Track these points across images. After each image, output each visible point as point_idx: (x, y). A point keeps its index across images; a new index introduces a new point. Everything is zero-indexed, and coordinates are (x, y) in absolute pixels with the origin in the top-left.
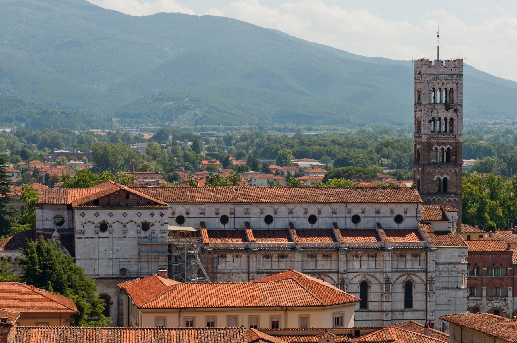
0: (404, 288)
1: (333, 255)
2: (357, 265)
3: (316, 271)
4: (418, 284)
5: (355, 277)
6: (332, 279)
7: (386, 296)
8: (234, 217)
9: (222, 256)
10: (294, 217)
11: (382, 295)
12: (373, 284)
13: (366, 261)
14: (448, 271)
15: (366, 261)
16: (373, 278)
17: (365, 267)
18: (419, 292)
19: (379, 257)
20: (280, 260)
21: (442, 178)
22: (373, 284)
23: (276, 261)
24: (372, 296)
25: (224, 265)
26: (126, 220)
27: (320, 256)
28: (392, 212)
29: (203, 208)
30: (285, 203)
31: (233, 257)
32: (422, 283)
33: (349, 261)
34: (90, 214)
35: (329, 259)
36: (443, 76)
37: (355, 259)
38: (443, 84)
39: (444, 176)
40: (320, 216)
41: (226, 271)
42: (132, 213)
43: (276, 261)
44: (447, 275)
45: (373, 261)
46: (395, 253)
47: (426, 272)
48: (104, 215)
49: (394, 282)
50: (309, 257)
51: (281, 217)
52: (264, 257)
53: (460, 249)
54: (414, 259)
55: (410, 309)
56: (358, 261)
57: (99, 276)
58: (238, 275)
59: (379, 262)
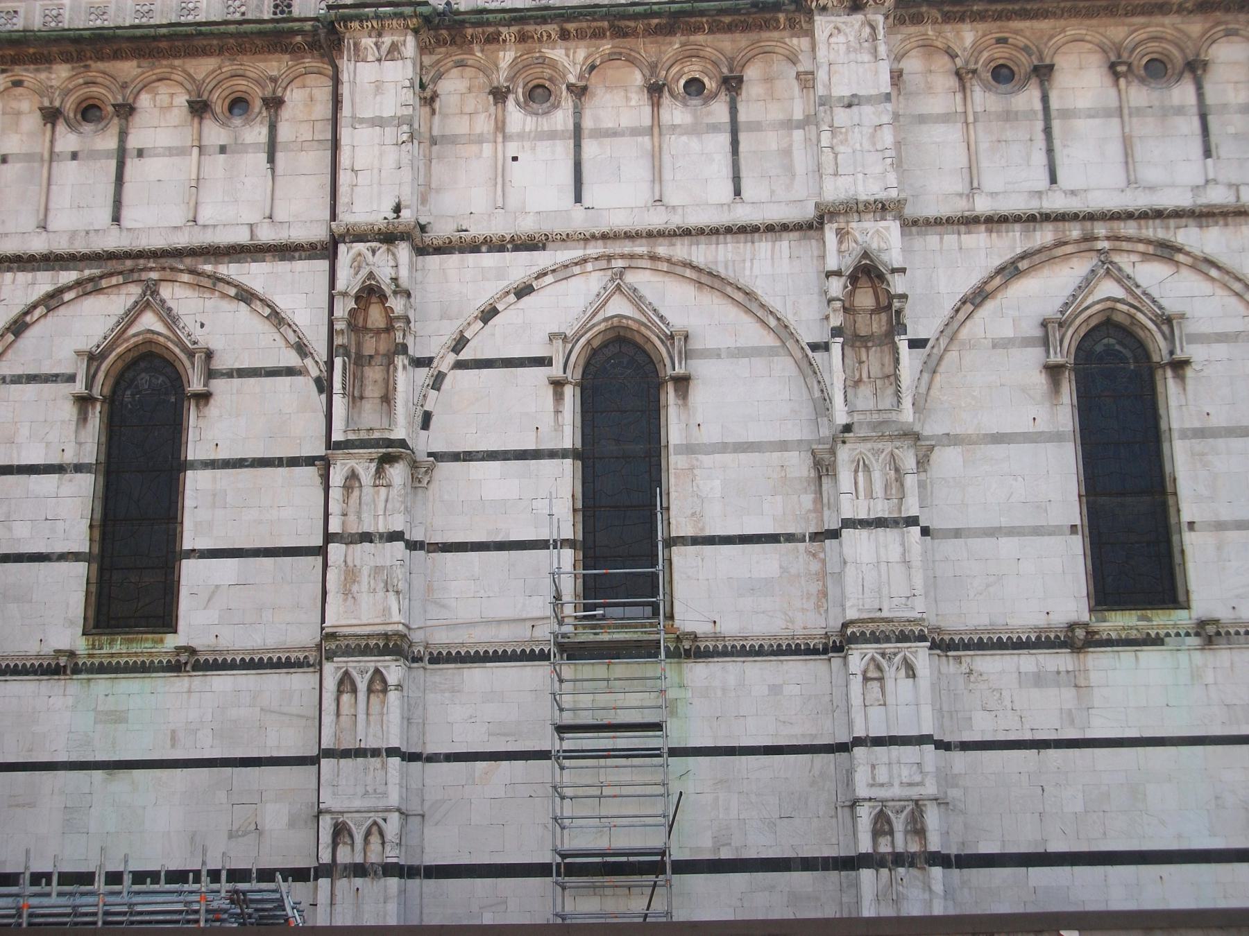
1: (295, 97)
3: (113, 241)
4: (1220, 350)
5: (523, 291)
6: (276, 318)
7: (862, 466)
11: (823, 468)
12: (716, 354)
13: (635, 132)
15: (635, 132)
19: (772, 96)
22: (716, 354)
33: (453, 140)
35: (257, 134)
37: (516, 117)
45: (694, 130)
46: (927, 47)
50: (51, 116)
54: (1138, 95)
55: (1161, 620)
56: (552, 135)
59: (772, 140)
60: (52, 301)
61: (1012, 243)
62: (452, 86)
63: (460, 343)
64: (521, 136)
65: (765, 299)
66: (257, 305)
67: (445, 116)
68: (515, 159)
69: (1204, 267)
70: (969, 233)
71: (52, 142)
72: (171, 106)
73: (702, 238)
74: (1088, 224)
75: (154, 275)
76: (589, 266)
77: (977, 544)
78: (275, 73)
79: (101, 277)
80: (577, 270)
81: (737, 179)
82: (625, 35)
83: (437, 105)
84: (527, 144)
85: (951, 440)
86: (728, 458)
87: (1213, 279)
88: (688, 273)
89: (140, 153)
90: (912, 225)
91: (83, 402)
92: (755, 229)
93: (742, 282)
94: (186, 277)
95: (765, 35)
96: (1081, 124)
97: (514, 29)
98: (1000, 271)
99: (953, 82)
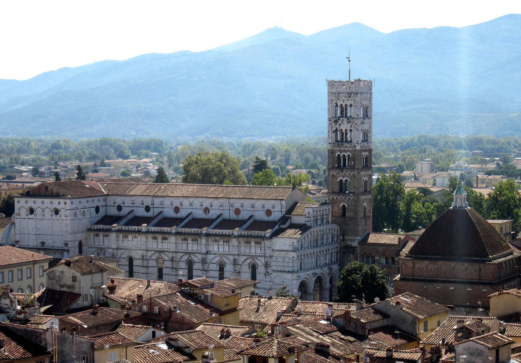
0: (251, 269)
2: (216, 248)
3: (187, 251)
8: (154, 207)
9: (126, 237)
17: (221, 250)
18: (261, 273)
20: (163, 241)
21: (344, 180)
24: (227, 274)
25: (126, 243)
26: (44, 206)
29: (133, 199)
30: (187, 197)
31: (132, 237)
34: (23, 200)
36: (343, 94)
38: (343, 100)
39: (345, 179)
40: (211, 208)
41: (127, 248)
42: (47, 201)
44: (281, 260)
45: (226, 245)
48: (31, 202)
49: (243, 263)
50: (182, 240)
53: (290, 239)
57: (29, 247)
62: (210, 240)
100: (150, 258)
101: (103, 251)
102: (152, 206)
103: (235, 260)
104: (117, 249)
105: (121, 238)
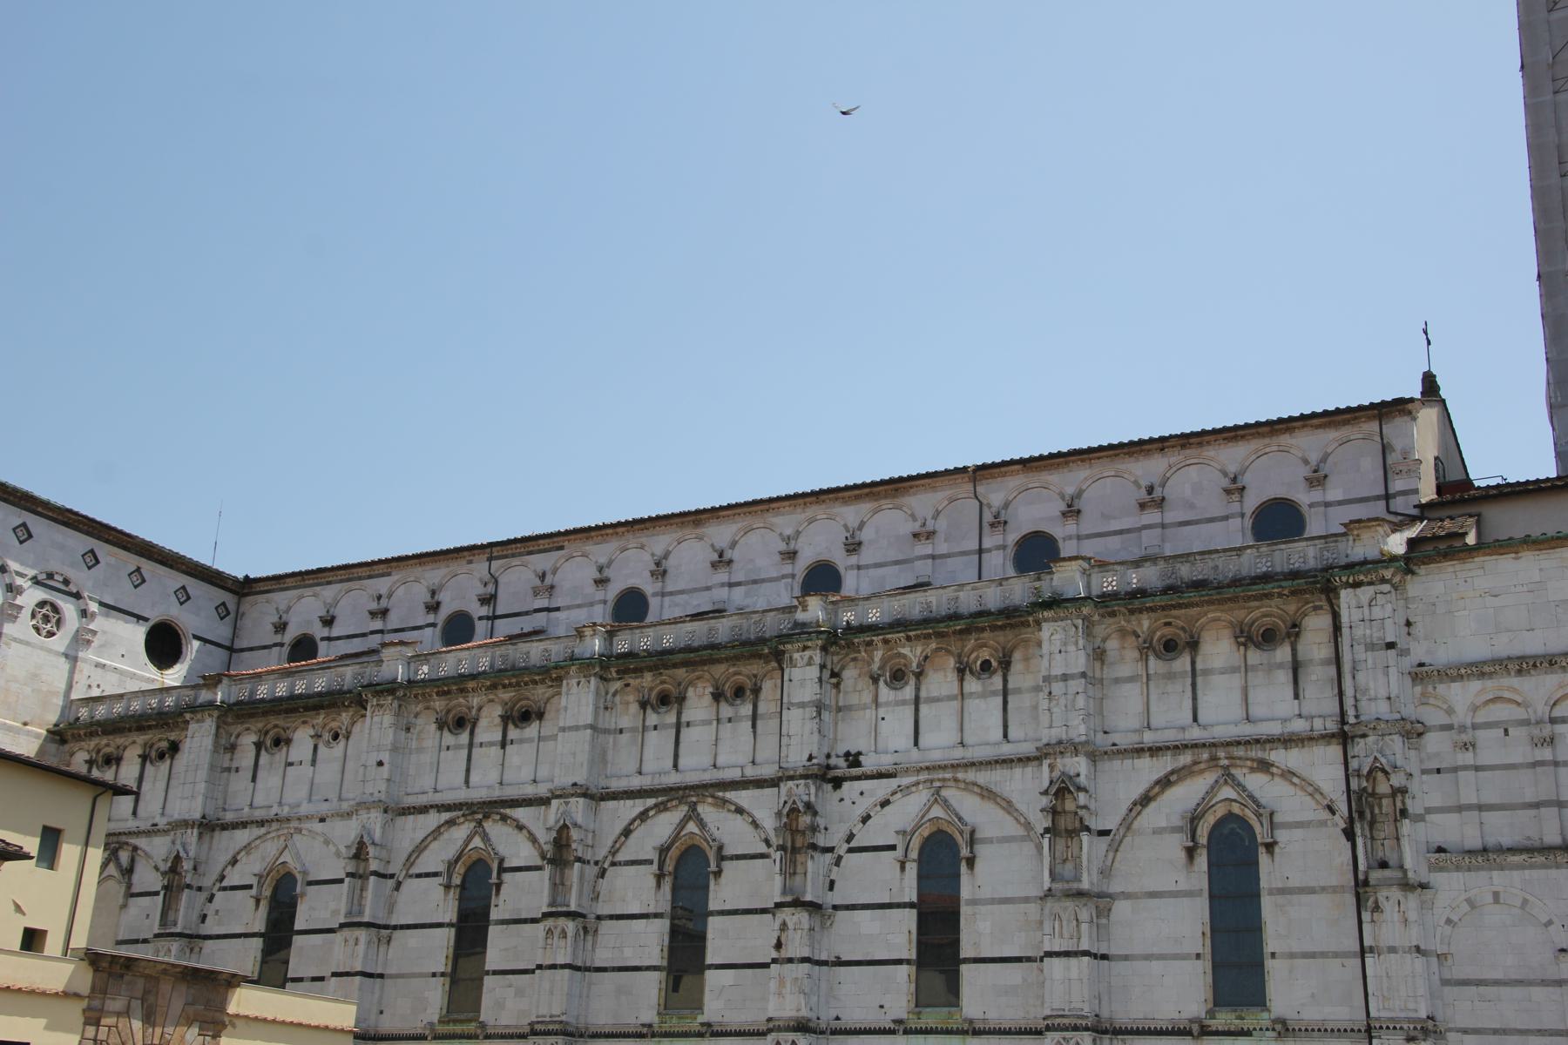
0: (1202, 860)
3: (673, 779)
4: (1298, 833)
5: (885, 803)
8: (495, 617)
10: (739, 584)
12: (990, 841)
13: (950, 698)
14: (1526, 723)
15: (950, 698)
16: (989, 807)
17: (940, 739)
18: (1311, 891)
20: (513, 733)
22: (990, 841)
23: (491, 744)
27: (701, 696)
28: (1235, 488)
29: (384, 591)
32: (1323, 823)
35: (746, 709)
37: (885, 693)
40: (853, 560)
43: (491, 744)
44: (1520, 751)
45: (983, 695)
47: (1344, 737)
49: (1127, 823)
50: (644, 705)
51: (682, 592)
52: (441, 725)
54: (1254, 656)
55: (1253, 1018)
56: (904, 702)
58: (318, 827)
60: (643, 816)
61: (1165, 764)
62: (849, 674)
63: (850, 837)
64: (887, 704)
65: (1018, 806)
66: (745, 816)
67: (846, 693)
68: (883, 719)
69: (1289, 776)
70: (1139, 758)
71: (644, 720)
72: (704, 694)
73: (983, 767)
74: (1214, 749)
75: (694, 799)
76: (921, 787)
77: (1138, 964)
78: (755, 672)
79: (668, 801)
80: (914, 789)
81: (1005, 727)
82: (943, 636)
83: (842, 687)
84: (890, 709)
85: (1126, 896)
86: (996, 907)
87: (1295, 785)
88: (976, 789)
89: (688, 724)
90: (1094, 756)
91: (659, 877)
92: (1012, 761)
93: (1005, 795)
94: (710, 800)
95: (1023, 630)
96: (1217, 680)
97: (881, 637)
98: (1158, 782)
99: (1136, 654)
100: (410, 861)
101: (124, 856)
102: (484, 611)
103: (1063, 789)
104: (208, 826)
105: (246, 757)
